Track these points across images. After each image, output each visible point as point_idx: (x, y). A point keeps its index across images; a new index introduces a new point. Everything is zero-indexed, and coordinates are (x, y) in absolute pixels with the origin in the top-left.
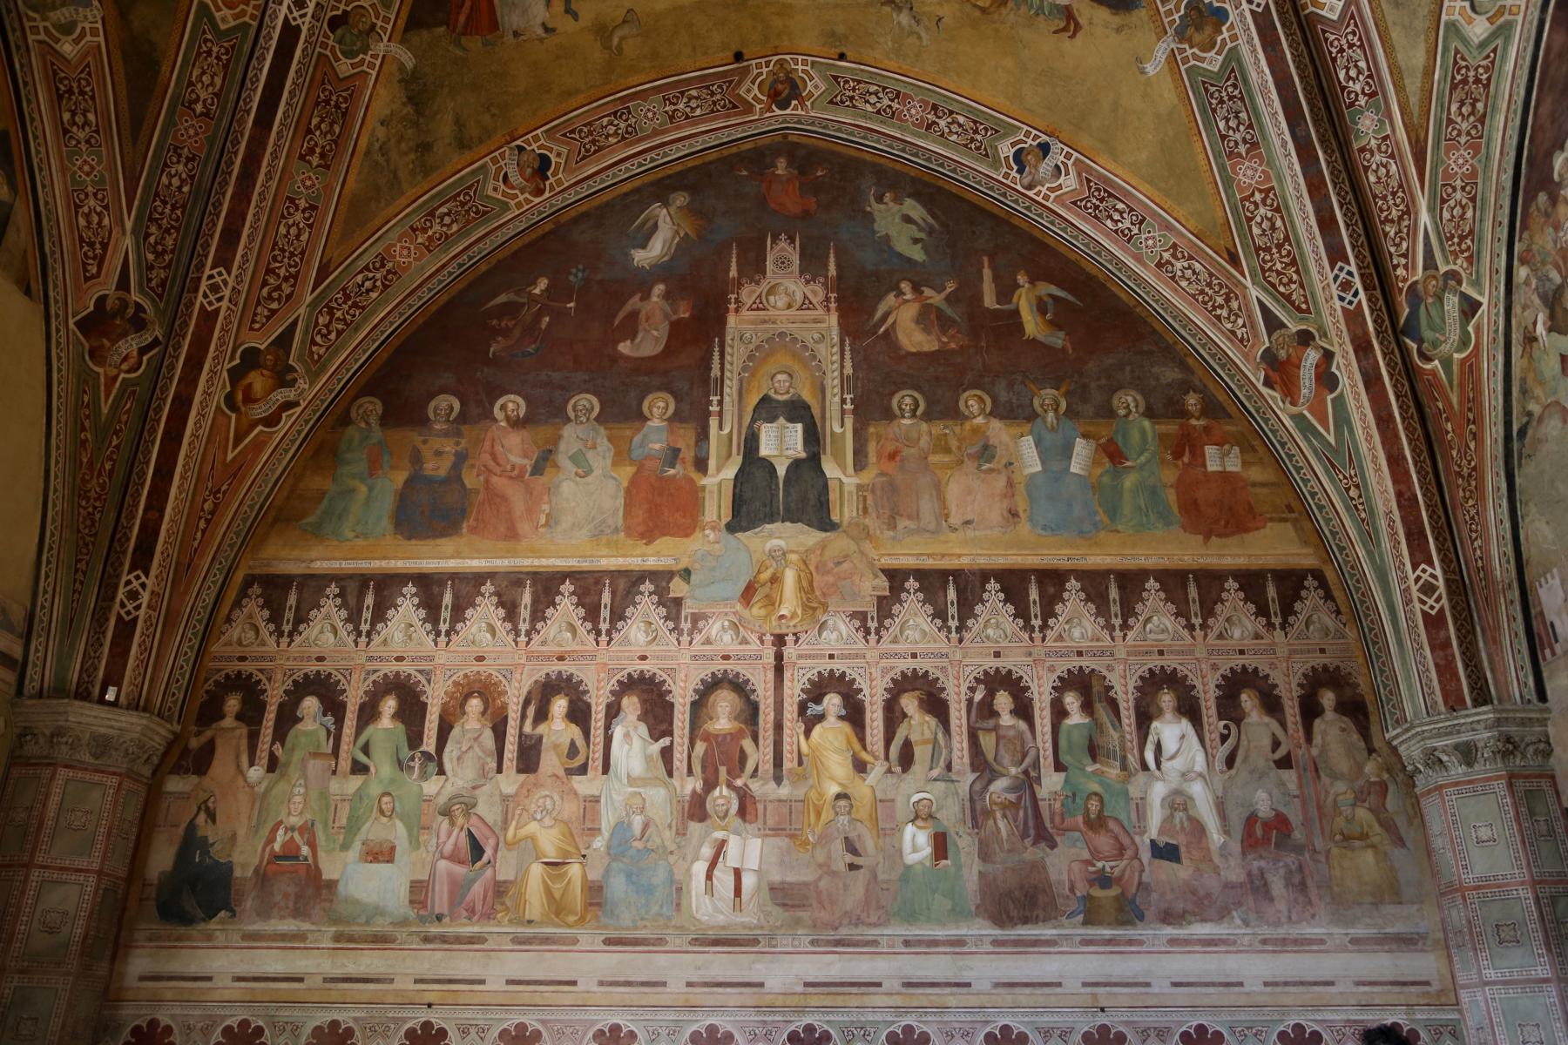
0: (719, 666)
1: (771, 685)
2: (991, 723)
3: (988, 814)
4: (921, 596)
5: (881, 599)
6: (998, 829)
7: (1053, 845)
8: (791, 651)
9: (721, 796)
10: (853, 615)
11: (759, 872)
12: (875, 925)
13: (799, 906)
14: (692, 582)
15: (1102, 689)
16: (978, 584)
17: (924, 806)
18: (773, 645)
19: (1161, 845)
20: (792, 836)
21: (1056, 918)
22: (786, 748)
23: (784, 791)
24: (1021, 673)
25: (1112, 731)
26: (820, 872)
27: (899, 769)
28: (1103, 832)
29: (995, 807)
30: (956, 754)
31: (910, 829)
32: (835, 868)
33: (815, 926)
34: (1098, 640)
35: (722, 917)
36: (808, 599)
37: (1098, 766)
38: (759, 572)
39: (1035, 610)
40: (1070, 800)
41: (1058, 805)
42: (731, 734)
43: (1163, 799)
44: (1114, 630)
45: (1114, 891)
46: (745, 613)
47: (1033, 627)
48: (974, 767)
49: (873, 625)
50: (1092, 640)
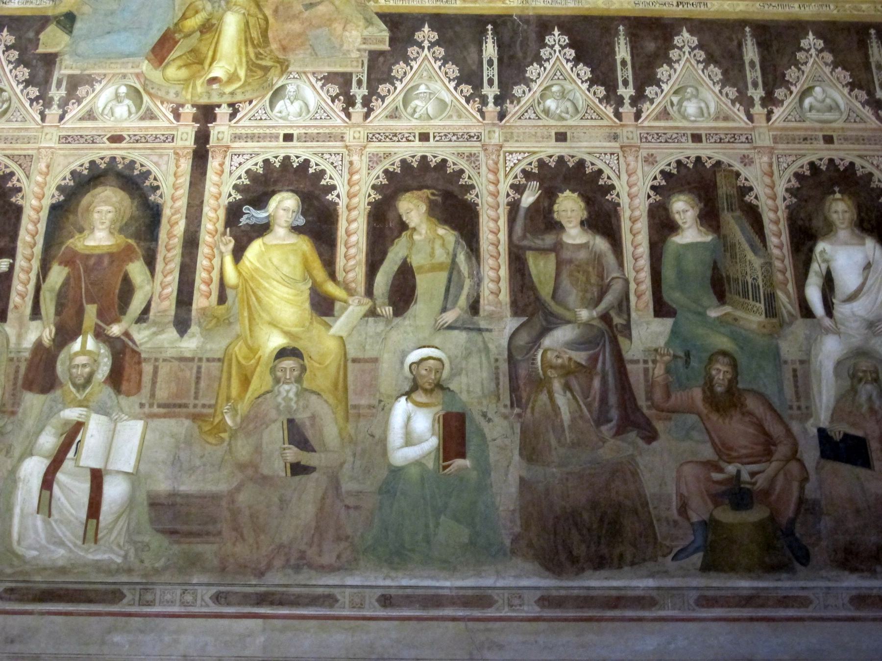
0: (103, 152)
1: (185, 180)
2: (549, 239)
3: (540, 383)
4: (440, 51)
5: (375, 57)
6: (556, 409)
7: (651, 436)
8: (224, 129)
9: (83, 351)
10: (329, 78)
11: (134, 477)
12: (331, 569)
13: (199, 535)
14: (76, 32)
15: (734, 191)
16: (533, 36)
17: (429, 370)
18: (195, 119)
19: (838, 437)
20: (195, 417)
21: (654, 559)
22: (201, 275)
23: (190, 344)
24: (600, 165)
25: (750, 256)
26: (240, 476)
27: (388, 310)
28: (737, 416)
29: (551, 373)
30: (487, 287)
31: (402, 407)
32: (266, 471)
33: (223, 570)
34: (726, 118)
35: (62, 552)
36: (258, 55)
37: (727, 309)
38: (184, 17)
39: (625, 73)
40: (680, 363)
41: (659, 371)
42: (111, 255)
43: (839, 364)
44: (753, 105)
45: (755, 515)
46: (155, 75)
47: (621, 98)
48: (517, 309)
49: (359, 92)
50: (717, 119)
